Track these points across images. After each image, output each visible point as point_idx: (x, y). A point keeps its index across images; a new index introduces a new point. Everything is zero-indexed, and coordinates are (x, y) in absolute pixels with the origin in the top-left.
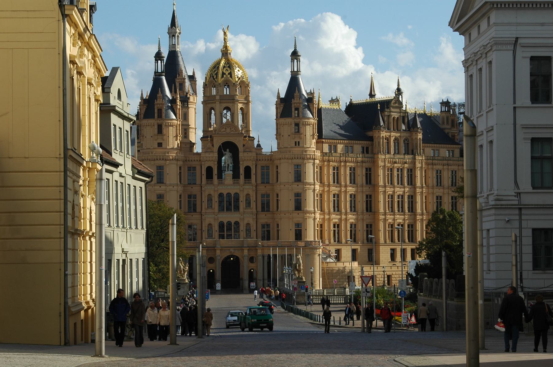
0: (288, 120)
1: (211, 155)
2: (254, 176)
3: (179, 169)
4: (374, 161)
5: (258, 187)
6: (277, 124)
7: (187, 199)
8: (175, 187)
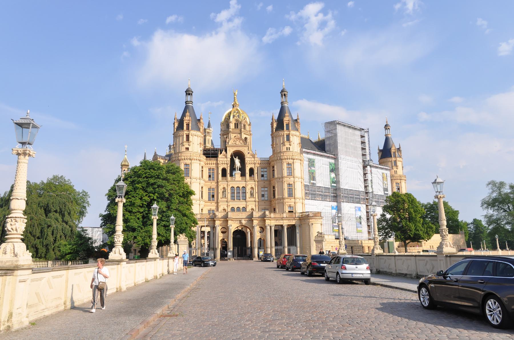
0: (281, 133)
1: (225, 159)
3: (201, 167)
6: (273, 138)
7: (207, 191)
8: (198, 180)
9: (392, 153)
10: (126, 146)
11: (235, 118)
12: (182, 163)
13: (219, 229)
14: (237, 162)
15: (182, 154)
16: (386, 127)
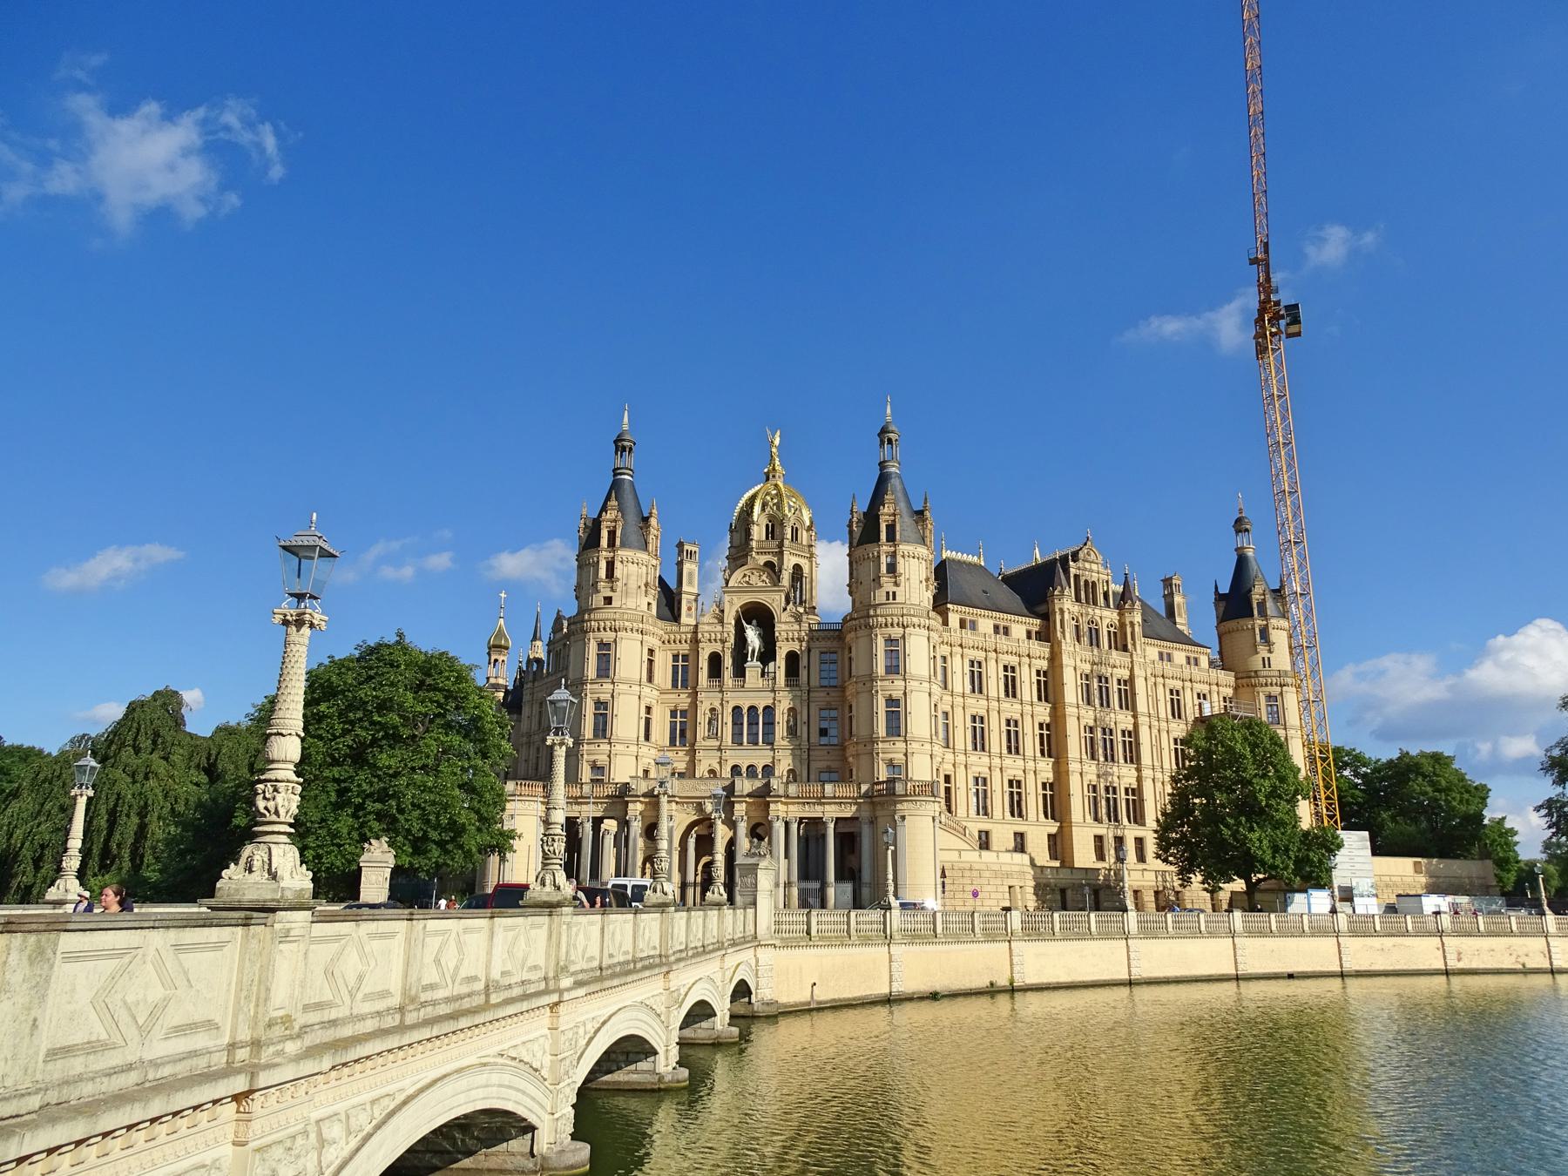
0: (871, 549)
1: (719, 628)
2: (805, 672)
3: (646, 651)
4: (1055, 658)
5: (811, 694)
6: (851, 564)
9: (1255, 605)
10: (503, 595)
11: (768, 510)
12: (592, 640)
13: (636, 827)
14: (753, 636)
15: (592, 616)
16: (1240, 526)
